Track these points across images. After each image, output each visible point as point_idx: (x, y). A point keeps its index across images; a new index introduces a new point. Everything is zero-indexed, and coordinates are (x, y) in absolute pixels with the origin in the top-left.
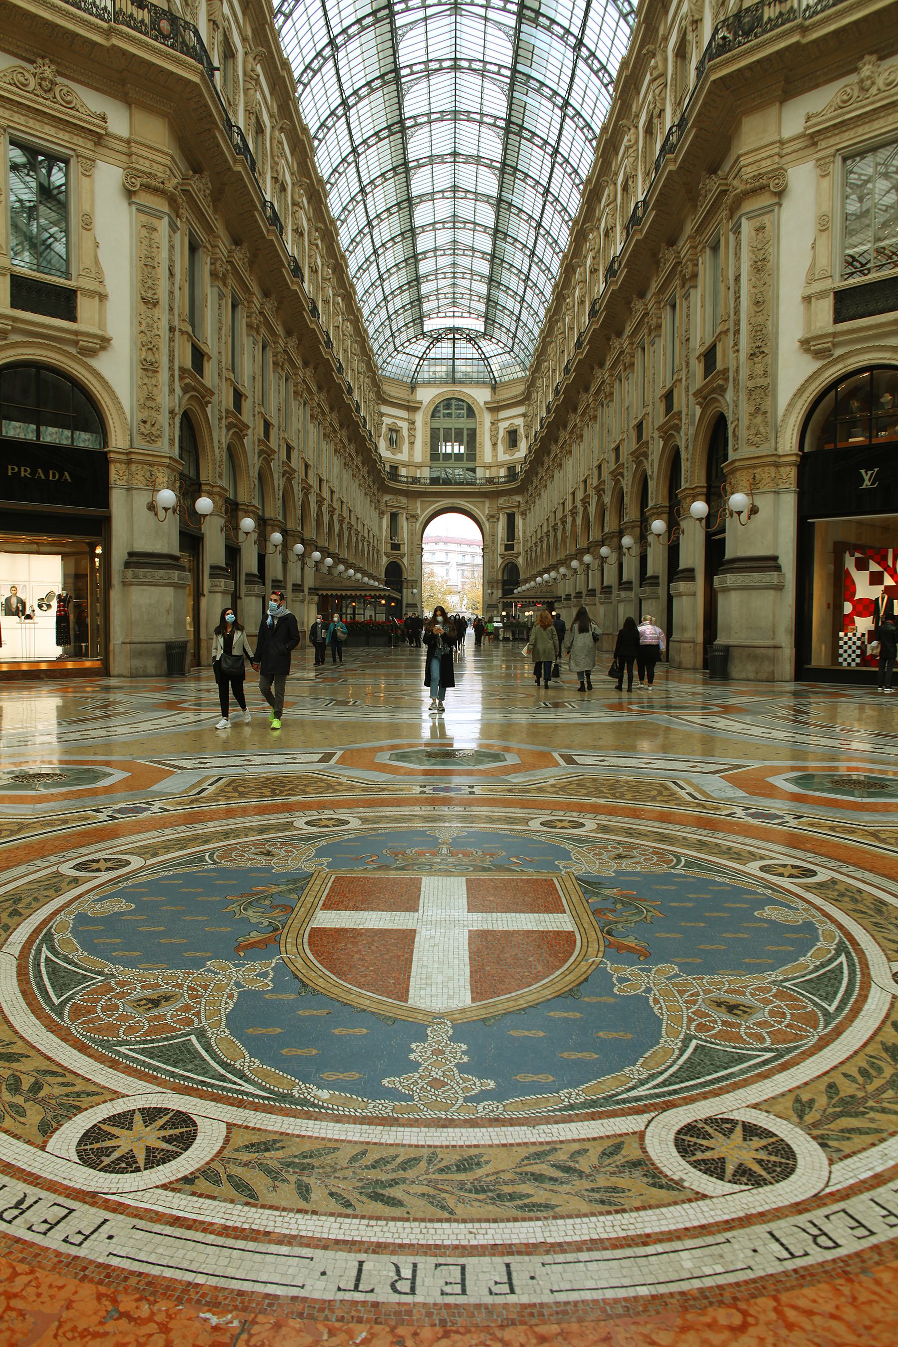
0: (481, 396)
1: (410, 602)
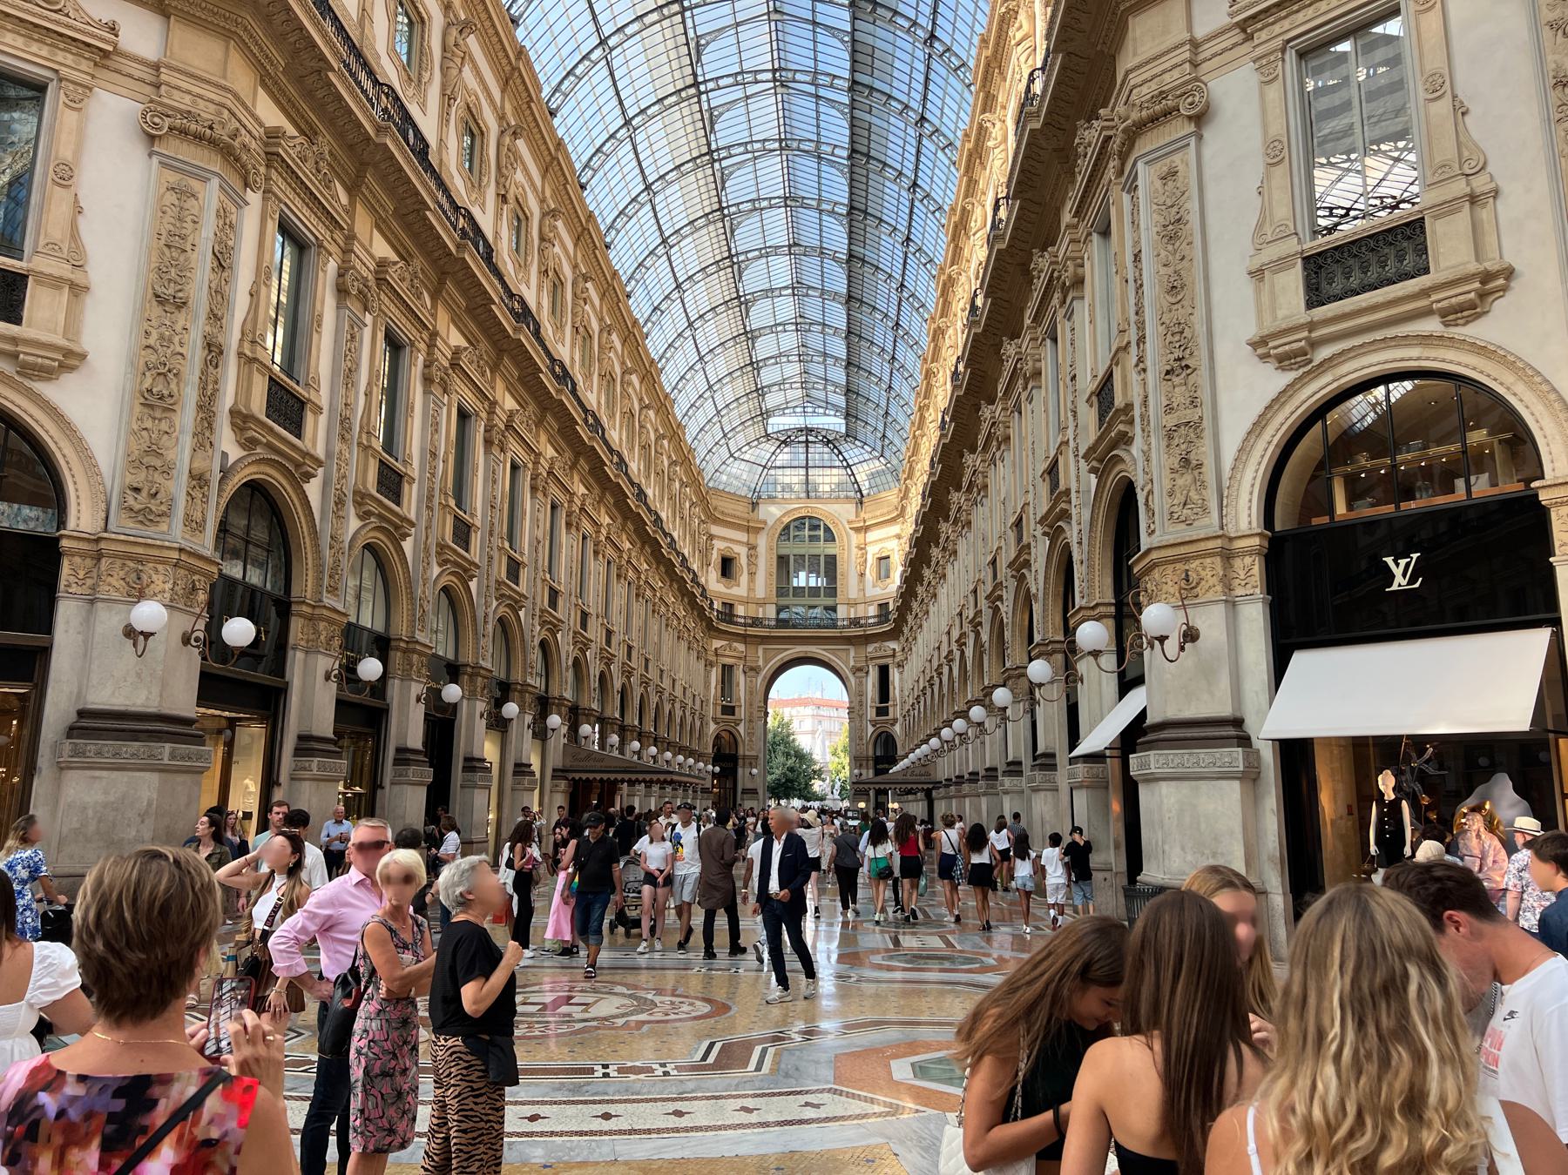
1: (749, 785)
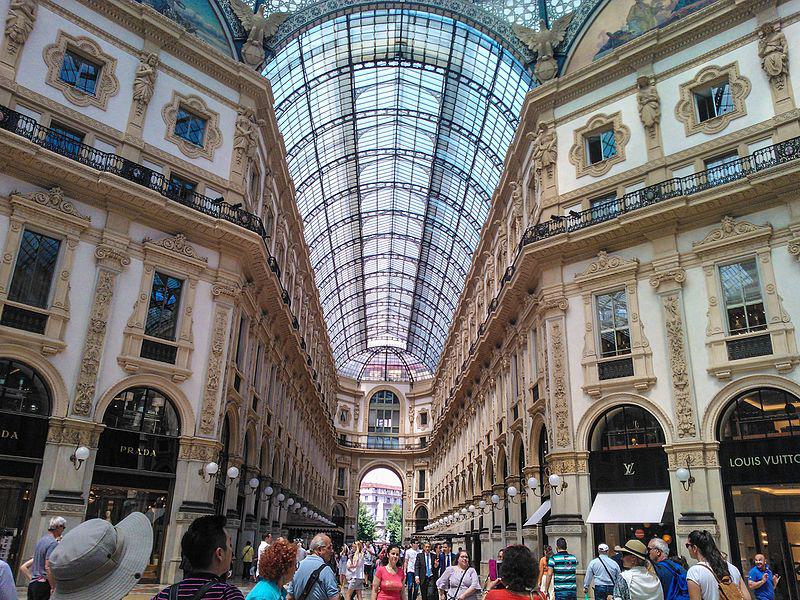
0: (403, 390)
